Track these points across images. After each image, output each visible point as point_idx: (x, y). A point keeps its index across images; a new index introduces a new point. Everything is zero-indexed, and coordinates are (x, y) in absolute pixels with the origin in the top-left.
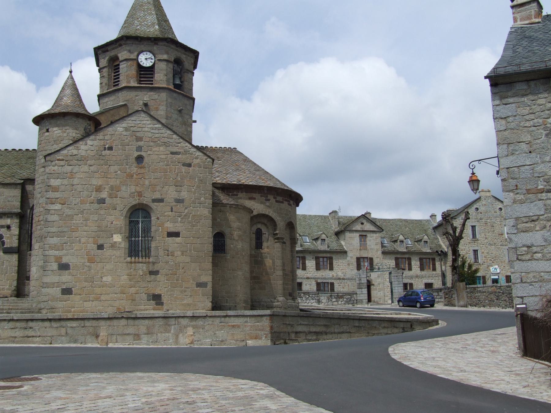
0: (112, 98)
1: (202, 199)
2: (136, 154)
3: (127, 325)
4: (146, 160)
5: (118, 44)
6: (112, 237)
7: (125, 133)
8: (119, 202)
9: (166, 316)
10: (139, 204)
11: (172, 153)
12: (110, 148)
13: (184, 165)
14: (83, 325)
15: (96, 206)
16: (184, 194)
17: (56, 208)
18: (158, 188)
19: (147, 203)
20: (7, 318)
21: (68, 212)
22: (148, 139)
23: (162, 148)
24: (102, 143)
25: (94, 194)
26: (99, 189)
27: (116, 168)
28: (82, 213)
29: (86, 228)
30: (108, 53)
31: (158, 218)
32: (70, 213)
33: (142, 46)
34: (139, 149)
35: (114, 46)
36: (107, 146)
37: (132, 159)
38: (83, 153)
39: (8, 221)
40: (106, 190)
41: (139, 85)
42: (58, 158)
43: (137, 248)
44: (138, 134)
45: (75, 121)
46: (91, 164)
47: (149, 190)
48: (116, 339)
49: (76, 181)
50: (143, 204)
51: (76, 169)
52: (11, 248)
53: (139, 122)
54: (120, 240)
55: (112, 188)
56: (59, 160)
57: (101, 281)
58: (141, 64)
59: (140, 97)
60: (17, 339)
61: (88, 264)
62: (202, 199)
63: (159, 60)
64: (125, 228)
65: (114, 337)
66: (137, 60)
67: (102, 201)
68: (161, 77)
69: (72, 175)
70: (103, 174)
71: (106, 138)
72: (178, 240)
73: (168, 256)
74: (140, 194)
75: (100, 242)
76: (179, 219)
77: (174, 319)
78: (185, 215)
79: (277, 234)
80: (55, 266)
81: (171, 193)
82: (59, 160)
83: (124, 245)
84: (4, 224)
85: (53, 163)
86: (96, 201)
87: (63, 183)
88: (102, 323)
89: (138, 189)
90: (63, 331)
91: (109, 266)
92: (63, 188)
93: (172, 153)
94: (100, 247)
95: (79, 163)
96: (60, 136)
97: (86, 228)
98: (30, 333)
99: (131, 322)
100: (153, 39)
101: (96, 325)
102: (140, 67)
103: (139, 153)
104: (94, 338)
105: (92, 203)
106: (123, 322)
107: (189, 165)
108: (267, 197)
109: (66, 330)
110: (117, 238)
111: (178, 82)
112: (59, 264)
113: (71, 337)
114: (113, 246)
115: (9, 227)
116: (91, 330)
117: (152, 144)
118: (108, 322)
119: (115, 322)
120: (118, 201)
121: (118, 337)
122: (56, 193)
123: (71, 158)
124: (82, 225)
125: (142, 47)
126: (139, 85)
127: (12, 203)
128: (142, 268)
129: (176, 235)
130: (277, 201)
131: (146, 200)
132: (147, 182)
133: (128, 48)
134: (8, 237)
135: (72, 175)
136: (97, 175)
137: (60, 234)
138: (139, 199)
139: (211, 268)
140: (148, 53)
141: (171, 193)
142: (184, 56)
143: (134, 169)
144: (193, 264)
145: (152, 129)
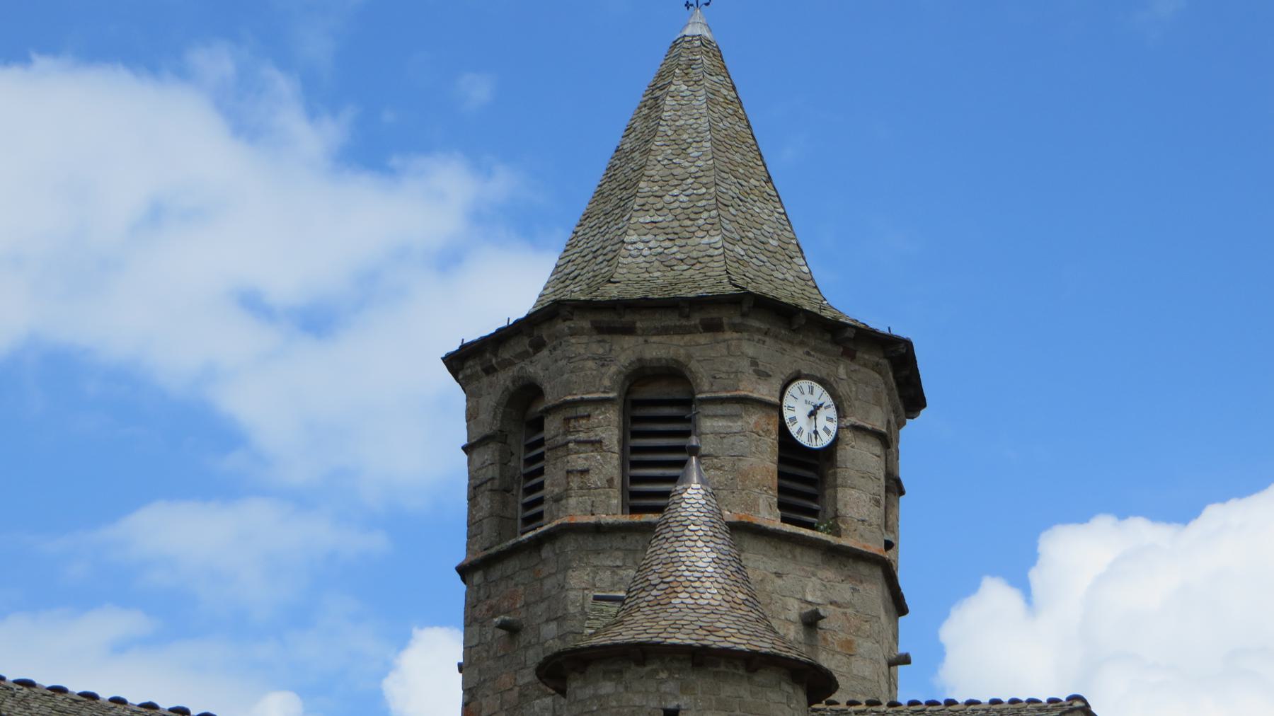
5: (695, 320)
30: (628, 342)
35: (672, 320)
41: (789, 528)
58: (793, 430)
63: (857, 429)
66: (779, 408)
100: (850, 334)
125: (796, 357)
126: (789, 528)
133: (750, 349)
140: (818, 389)
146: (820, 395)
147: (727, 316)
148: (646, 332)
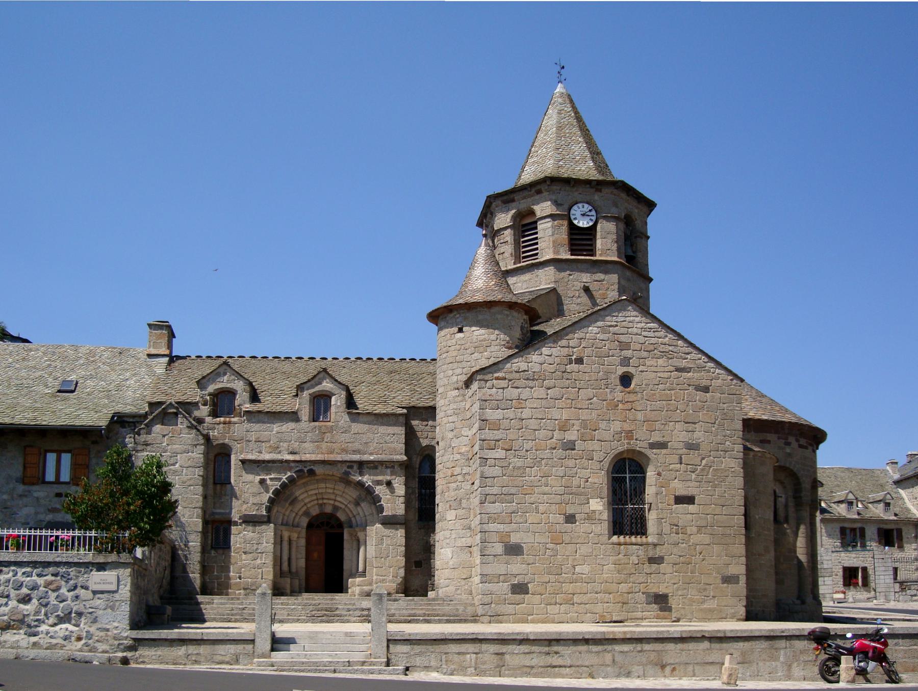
0: (527, 277)
2: (621, 370)
3: (711, 649)
5: (533, 190)
6: (588, 503)
9: (772, 634)
10: (628, 451)
11: (678, 370)
12: (579, 361)
13: (698, 388)
16: (699, 435)
18: (658, 425)
20: (518, 637)
21: (518, 462)
22: (638, 347)
23: (660, 362)
24: (565, 351)
25: (557, 434)
27: (590, 392)
29: (546, 489)
30: (514, 204)
32: (519, 464)
33: (576, 194)
35: (526, 193)
37: (615, 379)
38: (537, 368)
41: (573, 257)
44: (623, 338)
45: (507, 315)
46: (549, 386)
48: (694, 671)
49: (526, 413)
50: (634, 451)
51: (526, 393)
52: (394, 516)
54: (601, 508)
55: (584, 424)
56: (497, 378)
57: (574, 574)
60: (534, 671)
61: (551, 546)
62: (728, 443)
65: (690, 668)
67: (570, 446)
68: (606, 245)
71: (572, 343)
73: (677, 533)
74: (629, 435)
75: (570, 510)
76: (694, 476)
80: (499, 548)
81: (678, 435)
82: (497, 378)
85: (489, 384)
87: (506, 416)
88: (671, 646)
89: (627, 427)
90: (608, 657)
91: (584, 550)
93: (678, 370)
95: (531, 383)
96: (484, 340)
97: (546, 489)
100: (594, 183)
102: (573, 228)
103: (625, 369)
104: (658, 669)
105: (555, 448)
106: (706, 644)
107: (706, 389)
108: (787, 439)
109: (613, 655)
111: (630, 253)
113: (621, 668)
114: (590, 517)
115: (389, 484)
116: (653, 656)
117: (645, 354)
119: (692, 646)
120: (595, 445)
121: (697, 668)
124: (539, 484)
126: (573, 257)
127: (393, 445)
130: (800, 446)
132: (640, 416)
134: (389, 500)
135: (520, 403)
139: (744, 553)
141: (678, 435)
142: (636, 211)
143: (619, 393)
146: (587, 207)
147: (543, 187)
148: (519, 200)
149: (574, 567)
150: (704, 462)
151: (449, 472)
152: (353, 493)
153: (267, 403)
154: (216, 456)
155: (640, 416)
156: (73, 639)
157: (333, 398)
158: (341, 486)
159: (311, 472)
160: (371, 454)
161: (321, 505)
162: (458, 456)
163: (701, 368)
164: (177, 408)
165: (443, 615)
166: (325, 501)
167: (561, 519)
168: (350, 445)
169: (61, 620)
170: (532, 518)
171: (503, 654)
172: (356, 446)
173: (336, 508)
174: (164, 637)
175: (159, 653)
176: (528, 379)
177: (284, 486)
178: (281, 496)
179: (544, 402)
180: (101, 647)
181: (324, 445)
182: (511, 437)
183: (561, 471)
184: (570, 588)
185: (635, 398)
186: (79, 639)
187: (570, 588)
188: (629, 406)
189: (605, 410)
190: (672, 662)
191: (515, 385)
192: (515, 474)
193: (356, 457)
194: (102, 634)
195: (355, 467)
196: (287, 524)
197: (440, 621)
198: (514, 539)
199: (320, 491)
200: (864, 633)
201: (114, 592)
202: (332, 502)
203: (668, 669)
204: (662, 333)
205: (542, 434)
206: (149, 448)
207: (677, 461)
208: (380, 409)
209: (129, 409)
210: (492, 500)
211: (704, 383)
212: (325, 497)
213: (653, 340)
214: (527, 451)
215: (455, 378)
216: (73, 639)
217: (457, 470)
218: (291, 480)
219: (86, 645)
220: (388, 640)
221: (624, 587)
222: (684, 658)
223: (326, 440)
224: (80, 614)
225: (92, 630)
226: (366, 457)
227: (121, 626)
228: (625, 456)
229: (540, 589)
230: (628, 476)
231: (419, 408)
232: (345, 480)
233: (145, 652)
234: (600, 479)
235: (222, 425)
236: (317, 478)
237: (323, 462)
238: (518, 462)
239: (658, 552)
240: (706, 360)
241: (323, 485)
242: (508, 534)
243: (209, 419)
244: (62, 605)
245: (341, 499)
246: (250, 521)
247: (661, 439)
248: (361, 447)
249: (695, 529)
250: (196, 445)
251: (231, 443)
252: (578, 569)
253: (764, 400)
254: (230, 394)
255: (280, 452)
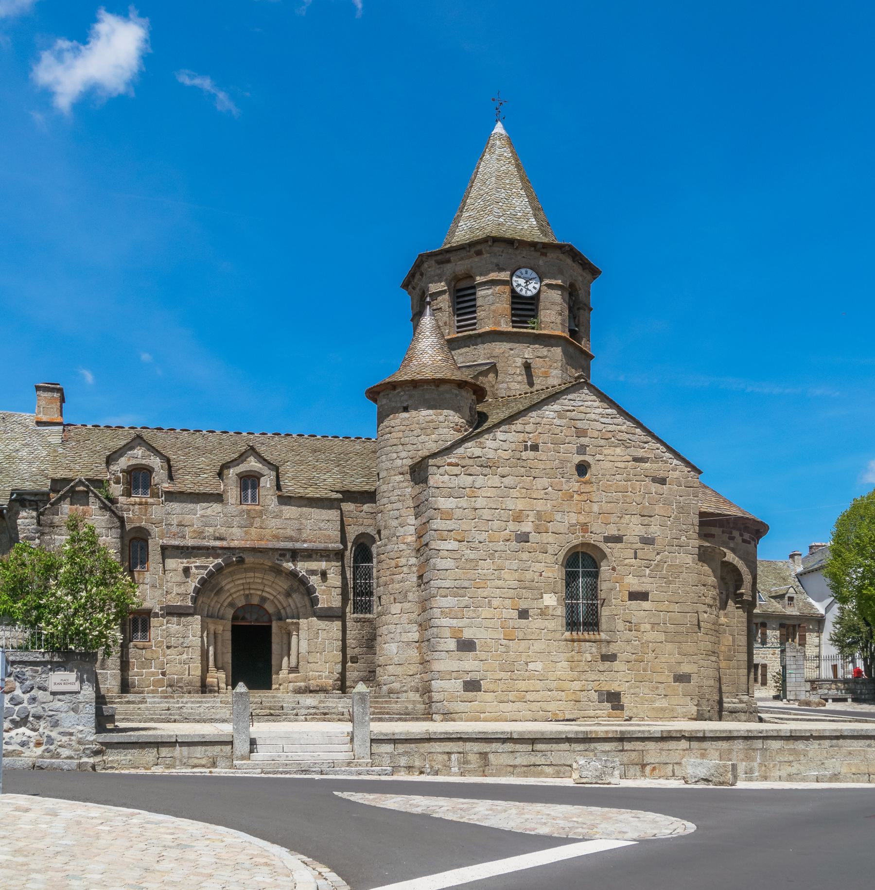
1: (683, 538)
2: (577, 459)
3: (690, 749)
4: (593, 470)
6: (542, 598)
7: (557, 421)
8: (551, 540)
9: (750, 734)
10: (583, 544)
11: (636, 460)
12: (535, 448)
13: (655, 480)
14: (621, 748)
15: (514, 545)
16: (655, 530)
17: (450, 547)
18: (613, 518)
19: (595, 543)
21: (471, 555)
23: (618, 450)
25: (512, 526)
26: (518, 518)
27: (545, 481)
28: (491, 556)
31: (614, 569)
32: (472, 556)
34: (582, 450)
36: (529, 443)
37: (571, 469)
38: (491, 454)
39: (323, 565)
40: (531, 519)
42: (449, 461)
43: (583, 619)
44: (579, 424)
45: (456, 395)
47: (600, 521)
48: (673, 771)
49: (480, 502)
50: (589, 545)
51: (480, 481)
53: (580, 403)
54: (555, 603)
55: (539, 515)
56: (449, 464)
59: (516, 351)
60: (518, 770)
61: (504, 642)
64: (561, 586)
67: (523, 538)
69: (473, 492)
70: (525, 491)
71: (528, 430)
72: (645, 605)
74: (585, 527)
75: (523, 605)
76: (648, 571)
77: (761, 741)
78: (657, 565)
79: (742, 594)
80: (452, 644)
81: (634, 528)
82: (449, 464)
83: (561, 611)
84: (315, 568)
85: (442, 470)
86: (513, 538)
88: (651, 745)
89: (582, 519)
91: (538, 646)
92: (458, 513)
93: (636, 460)
94: (524, 614)
96: (432, 421)
98: (538, 759)
99: (695, 744)
101: (641, 748)
106: (684, 744)
110: (550, 600)
112: (458, 641)
114: (543, 613)
115: (324, 575)
117: (603, 442)
118: (661, 745)
119: (672, 745)
122: (448, 522)
123: (471, 462)
124: (493, 577)
128: (590, 651)
129: (643, 596)
131: (595, 539)
132: (595, 508)
134: (324, 591)
136: (514, 493)
137: (458, 591)
138: (583, 536)
141: (634, 528)
144: (669, 646)
145: (603, 416)
149: (527, 664)
150: (659, 557)
151: (393, 563)
152: (283, 584)
153: (187, 483)
154: (130, 541)
155: (595, 508)
156: (32, 745)
157: (262, 479)
158: (270, 577)
159: (241, 561)
160: (305, 541)
161: (247, 596)
162: (403, 547)
163: (658, 459)
164: (87, 487)
165: (394, 714)
166: (252, 592)
167: (515, 614)
168: (282, 531)
169: (16, 724)
170: (485, 612)
171: (486, 754)
172: (289, 532)
173: (263, 599)
174: (134, 740)
175: (129, 757)
176: (482, 466)
177: (211, 575)
178: (208, 585)
179: (499, 490)
180: (65, 752)
181: (253, 531)
182: (465, 527)
183: (515, 564)
184: (522, 685)
185: (591, 489)
186: (38, 744)
187: (522, 685)
188: (584, 497)
189: (560, 501)
190: (652, 761)
191: (467, 472)
192: (468, 566)
193: (289, 545)
194: (65, 739)
195: (288, 556)
196: (212, 617)
197: (391, 720)
198: (467, 634)
199: (248, 581)
200: (839, 734)
201: (76, 693)
202: (259, 593)
203: (648, 769)
204: (620, 420)
205: (496, 524)
206: (57, 530)
207: (633, 556)
208: (311, 493)
209: (28, 486)
210: (443, 594)
211: (661, 474)
212: (252, 586)
213: (610, 428)
214: (480, 542)
215: (399, 462)
216: (32, 745)
217: (403, 561)
218: (219, 569)
219: (47, 750)
220: (372, 741)
221: (577, 685)
222: (664, 758)
223: (255, 525)
224: (38, 718)
225: (54, 734)
226: (298, 545)
227: (86, 729)
228: (579, 549)
229: (492, 687)
230: (581, 570)
231: (354, 492)
232: (278, 571)
233: (112, 757)
234: (556, 573)
235: (137, 507)
236: (244, 566)
237: (253, 550)
238: (471, 555)
239: (613, 649)
240: (665, 450)
241: (252, 575)
242: (460, 630)
243: (122, 499)
244: (17, 708)
245: (270, 591)
246: (172, 612)
247: (616, 533)
248: (293, 534)
249: (648, 626)
250: (111, 528)
251: (149, 527)
252: (531, 666)
253: (708, 491)
254: (147, 471)
255: (204, 538)
